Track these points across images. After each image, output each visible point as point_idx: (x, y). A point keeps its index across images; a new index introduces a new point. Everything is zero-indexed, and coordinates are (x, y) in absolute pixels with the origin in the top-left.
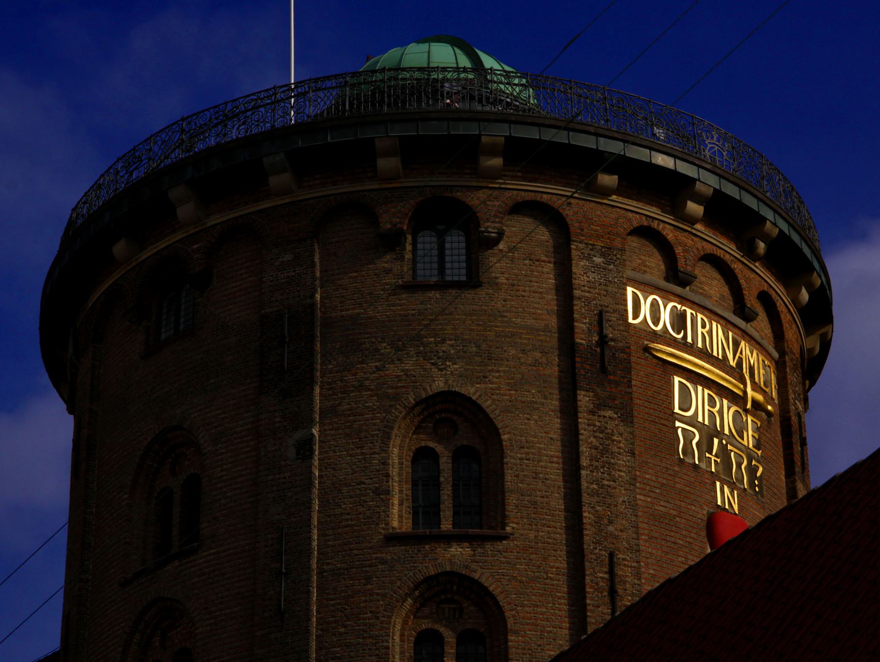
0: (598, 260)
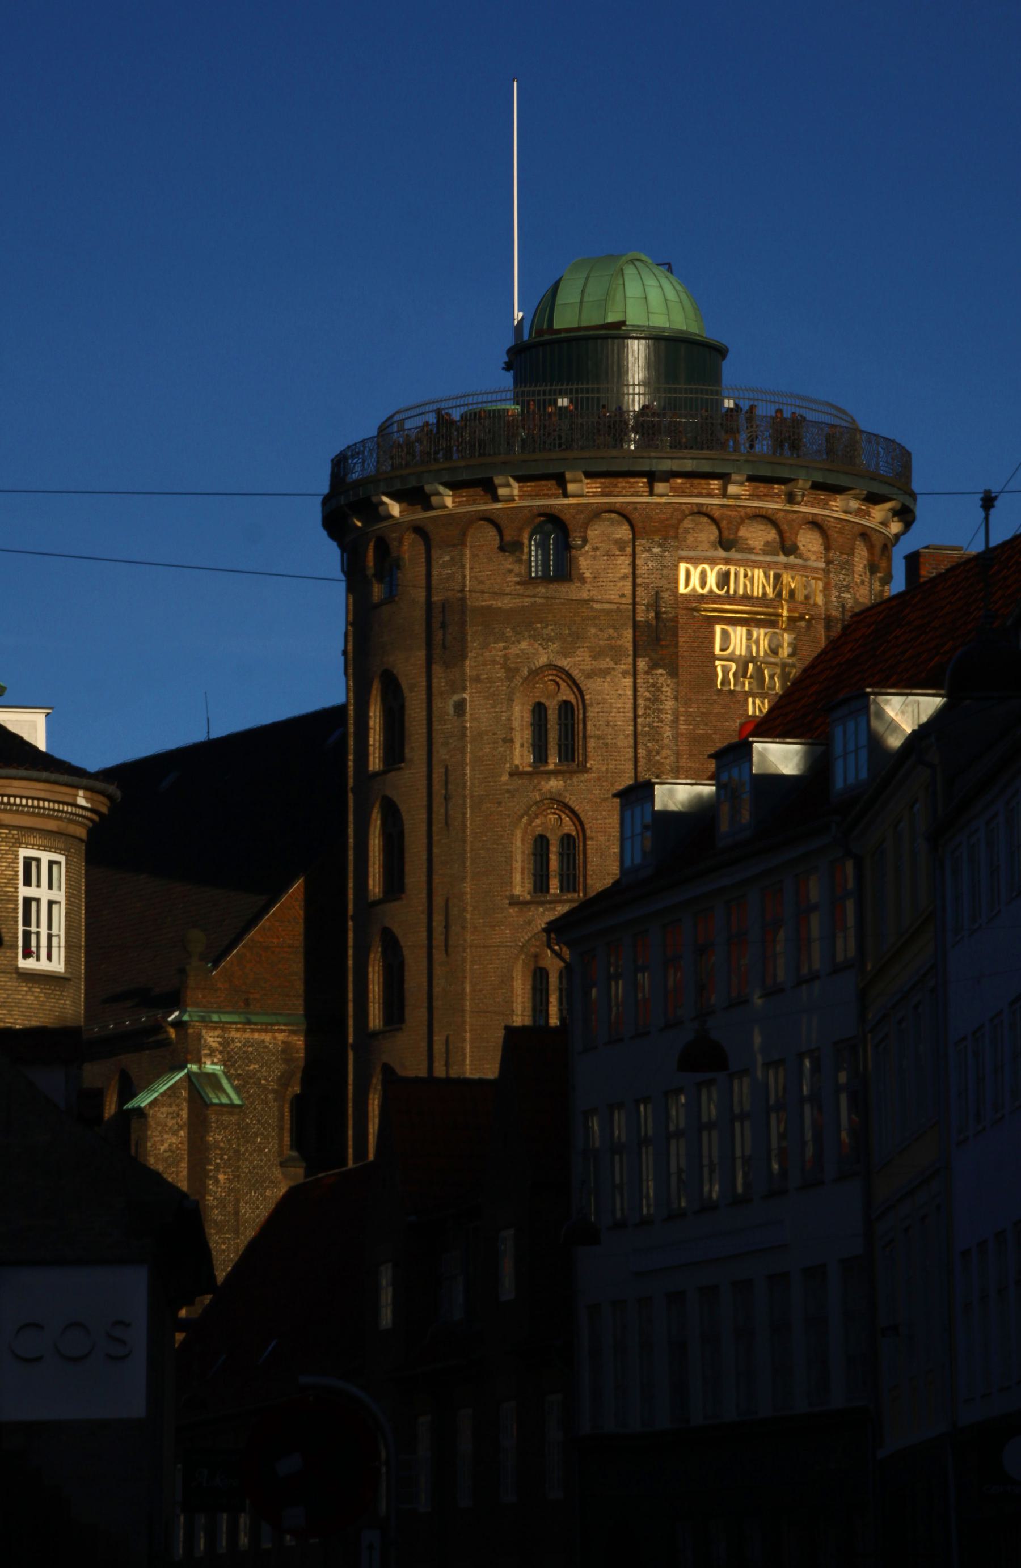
0: (656, 550)
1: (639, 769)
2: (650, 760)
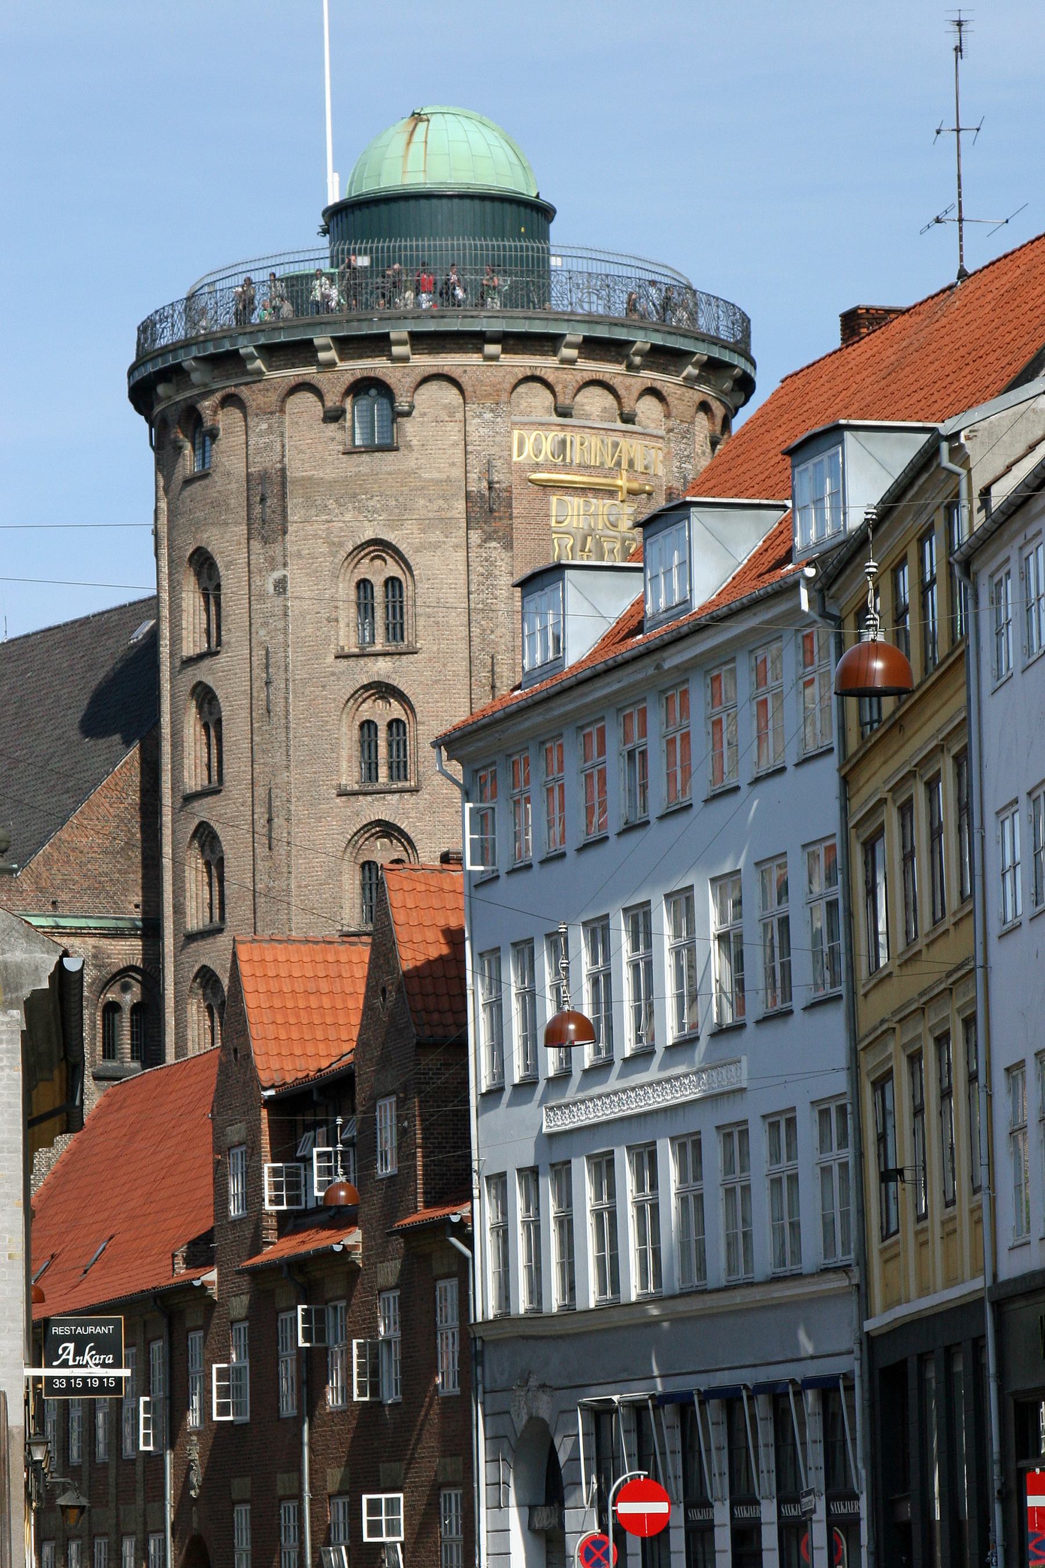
0: (488, 416)
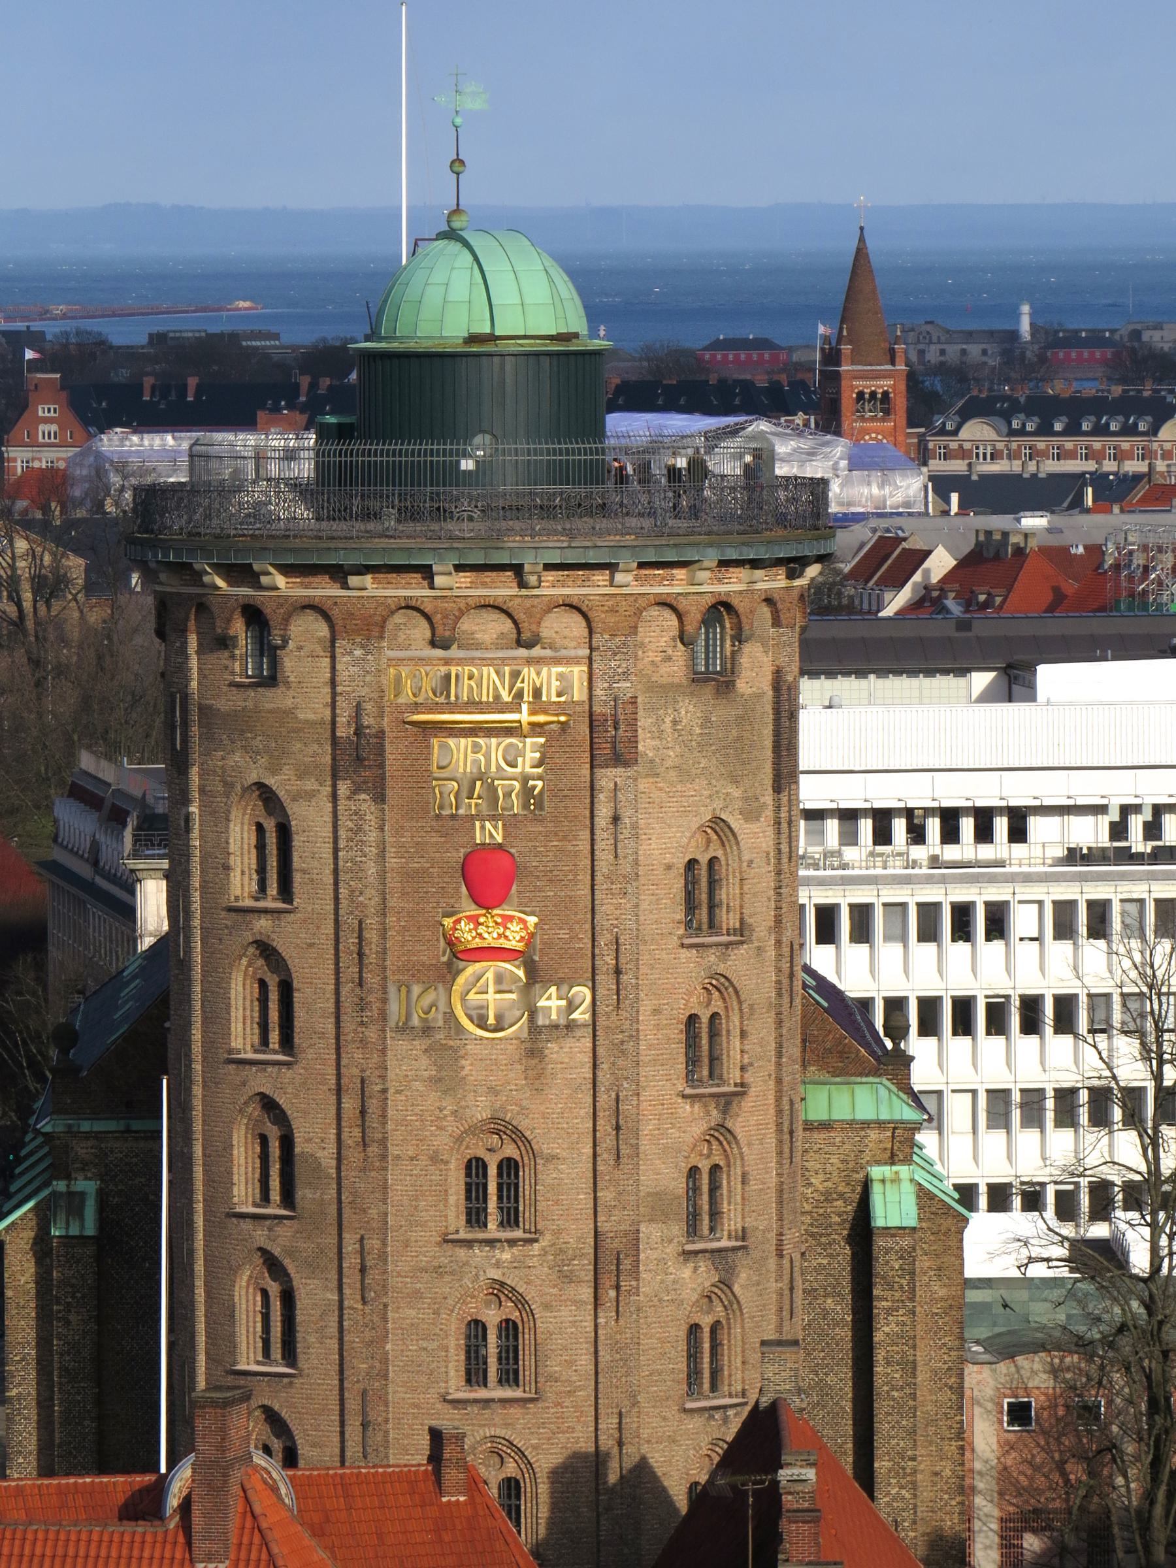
0: (358, 653)
1: (341, 912)
2: (353, 902)
